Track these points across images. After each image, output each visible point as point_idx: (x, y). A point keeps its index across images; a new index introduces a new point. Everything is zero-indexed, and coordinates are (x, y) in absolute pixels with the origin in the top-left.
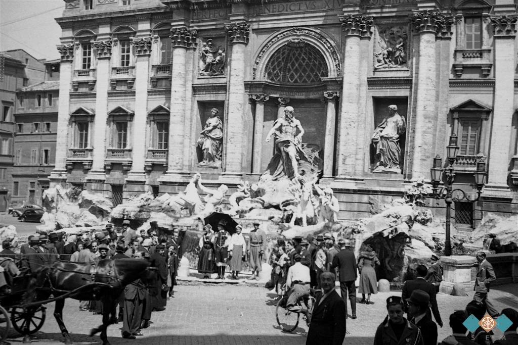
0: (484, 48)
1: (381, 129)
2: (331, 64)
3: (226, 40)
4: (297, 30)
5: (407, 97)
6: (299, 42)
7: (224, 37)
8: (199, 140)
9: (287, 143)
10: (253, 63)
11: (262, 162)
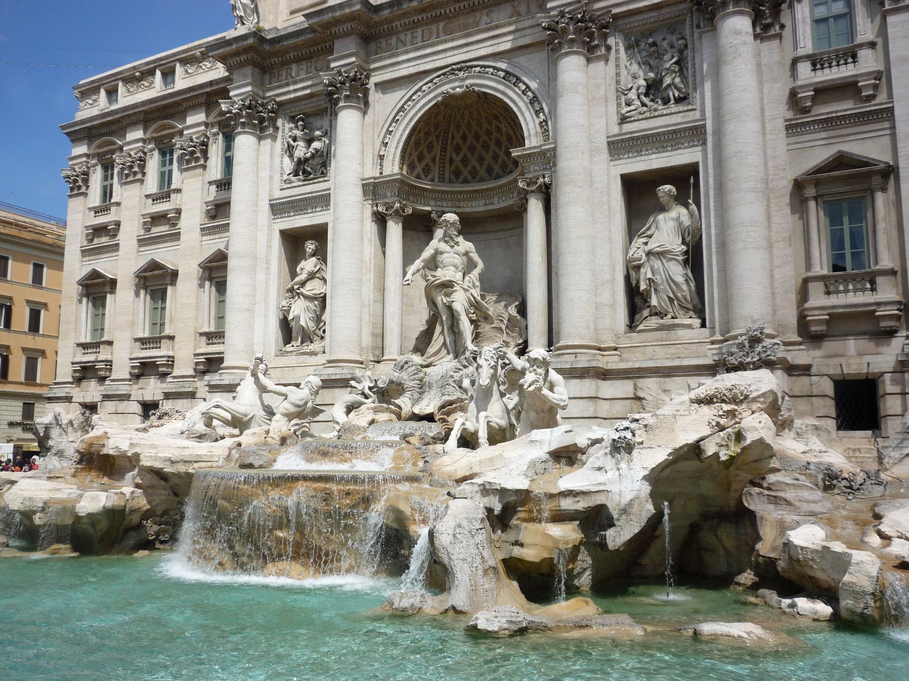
0: (859, 39)
1: (644, 240)
2: (529, 123)
4: (460, 70)
5: (697, 164)
6: (464, 96)
7: (326, 109)
8: (284, 303)
9: (447, 286)
10: (378, 144)
11: (403, 337)
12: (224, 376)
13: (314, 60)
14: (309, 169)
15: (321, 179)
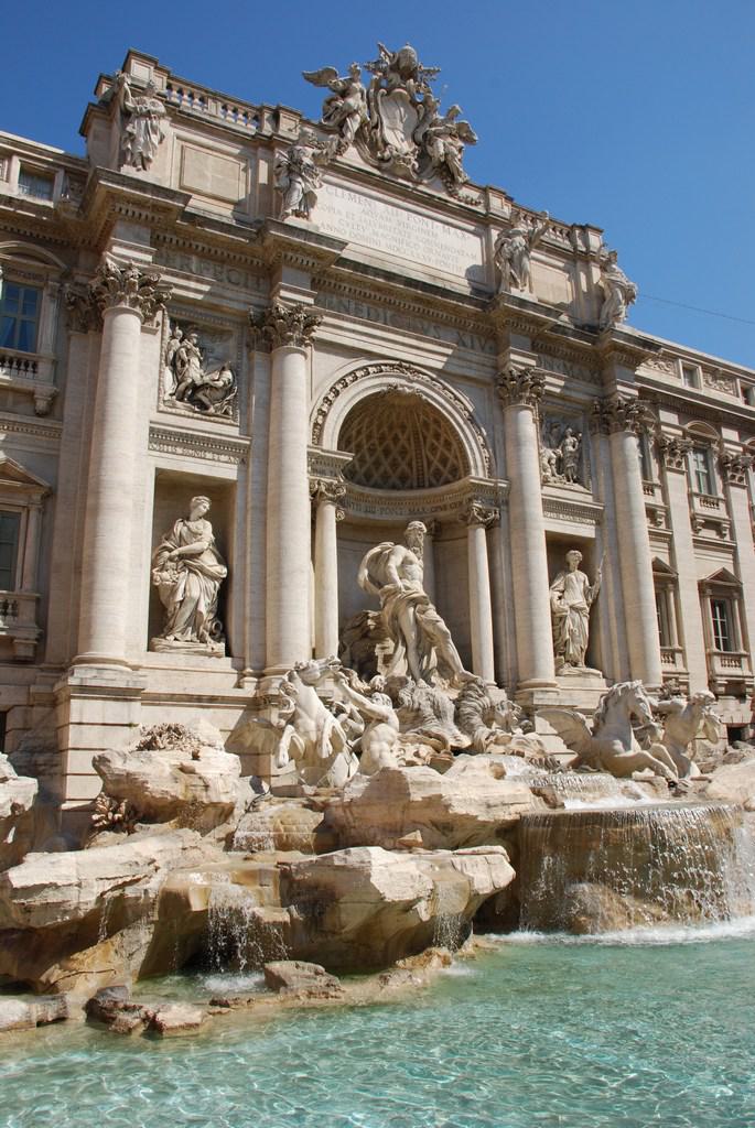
3: (232, 343)
4: (407, 369)
12: (107, 675)
13: (226, 267)
14: (204, 399)
15: (225, 420)
